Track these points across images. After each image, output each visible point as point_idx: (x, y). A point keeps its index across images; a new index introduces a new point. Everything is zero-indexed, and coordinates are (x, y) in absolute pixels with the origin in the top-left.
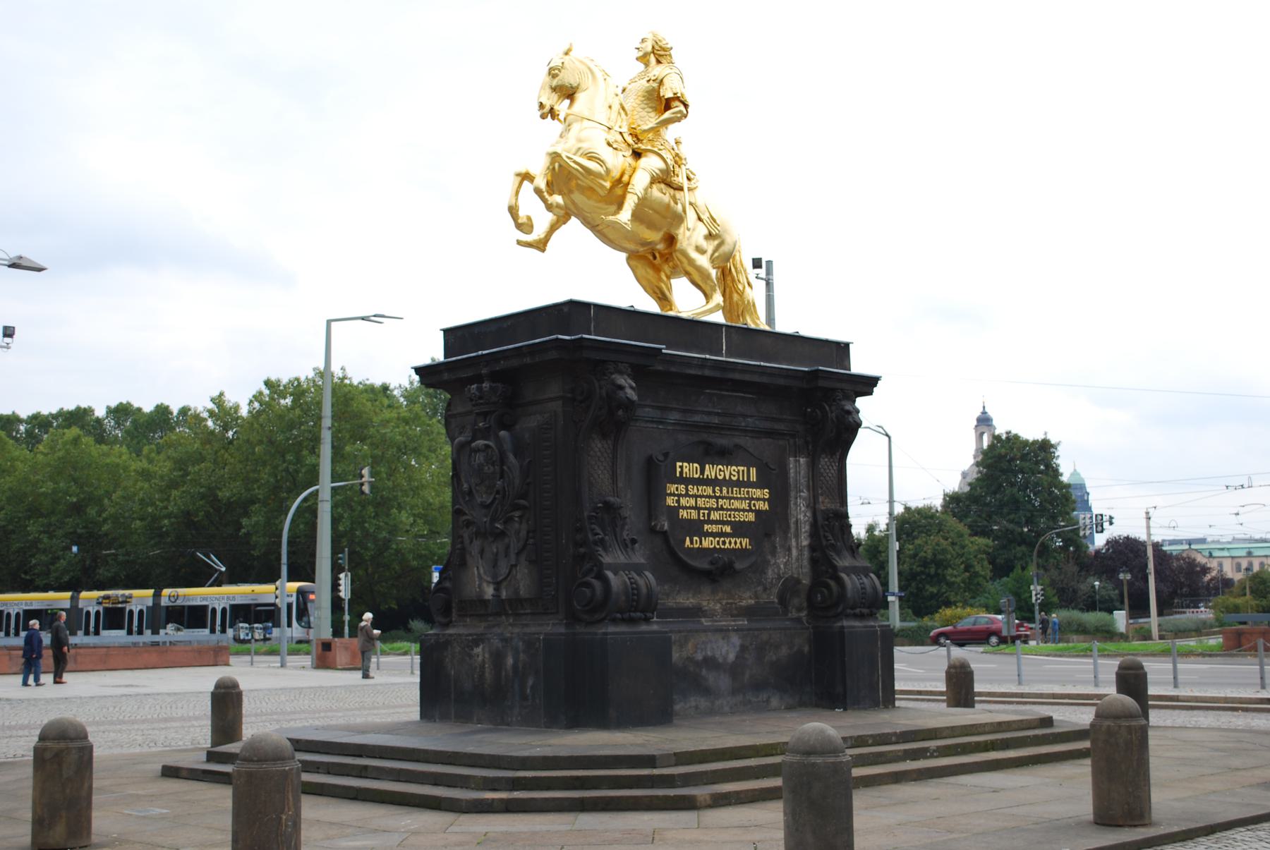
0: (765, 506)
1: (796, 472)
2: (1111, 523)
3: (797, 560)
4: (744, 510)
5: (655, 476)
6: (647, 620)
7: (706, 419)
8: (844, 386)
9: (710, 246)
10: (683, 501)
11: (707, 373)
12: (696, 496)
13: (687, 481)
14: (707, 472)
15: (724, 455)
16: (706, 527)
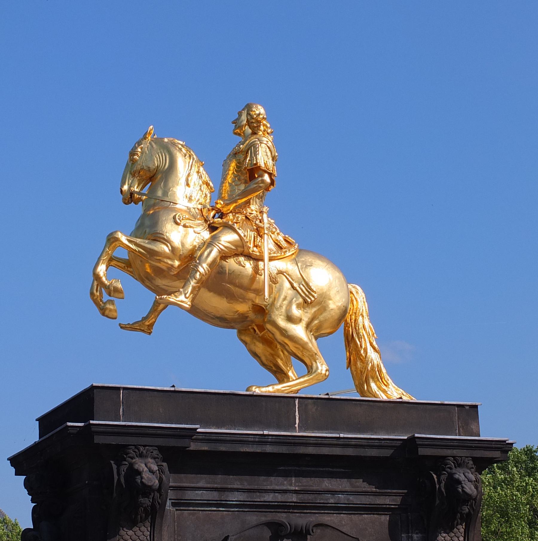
7: (280, 497)
8: (455, 452)
9: (305, 315)
11: (269, 449)
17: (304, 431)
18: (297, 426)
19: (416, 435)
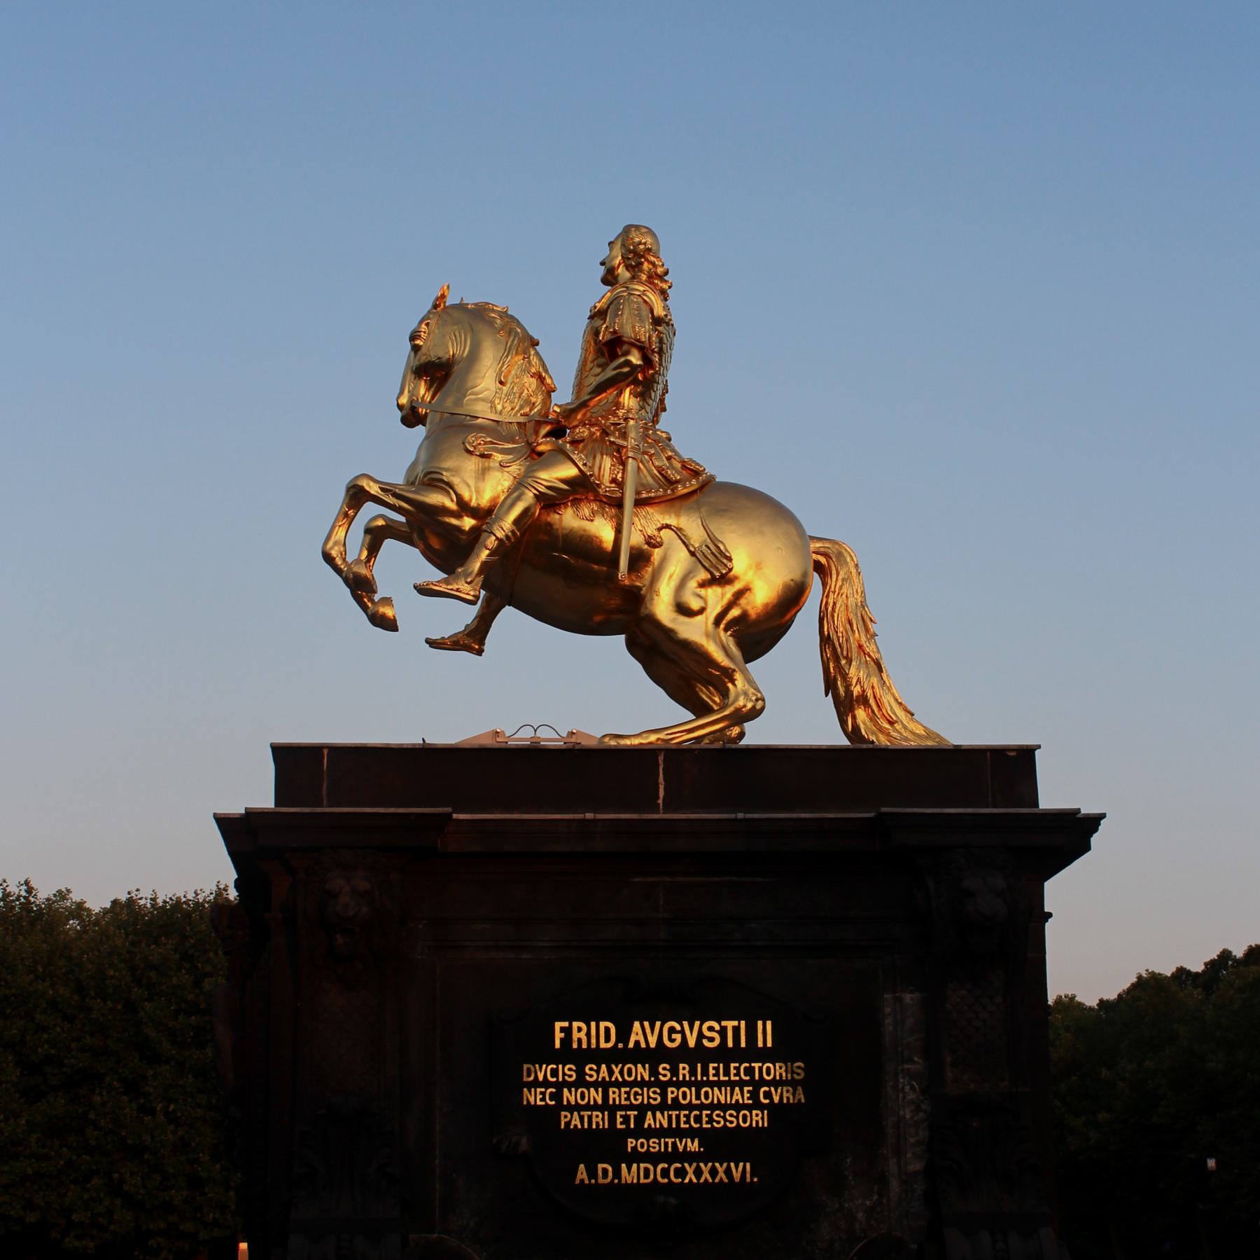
4: (738, 1107)
10: (569, 1096)
12: (605, 1086)
16: (631, 1143)
17: (675, 811)
18: (660, 801)
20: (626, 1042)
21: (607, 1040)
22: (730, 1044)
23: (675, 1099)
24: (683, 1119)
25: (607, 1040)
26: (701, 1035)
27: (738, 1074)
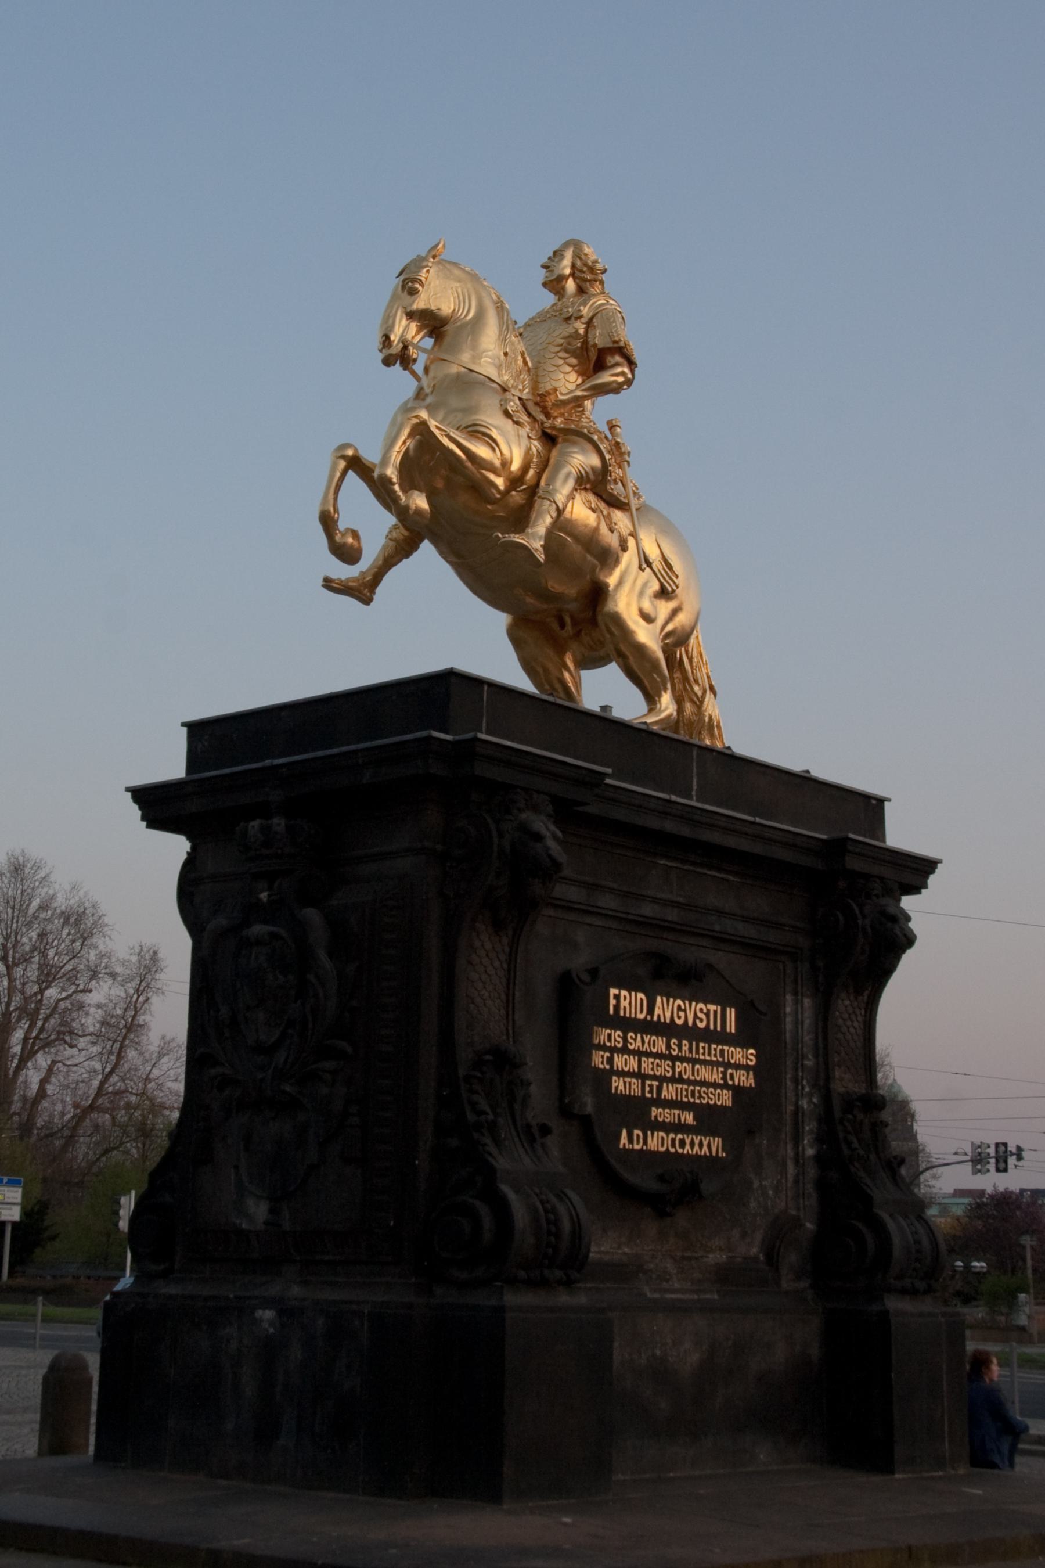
0: (744, 1079)
1: (796, 1023)
2: (1020, 1158)
3: (796, 1182)
4: (715, 1085)
5: (574, 1009)
6: (568, 1283)
10: (619, 1061)
11: (669, 826)
12: (639, 1054)
13: (627, 1024)
14: (658, 1011)
15: (687, 981)
19: (851, 836)
20: (652, 1017)
21: (641, 1012)
22: (712, 1027)
23: (680, 1073)
24: (684, 1093)
25: (641, 1012)
26: (696, 1016)
27: (715, 1055)
